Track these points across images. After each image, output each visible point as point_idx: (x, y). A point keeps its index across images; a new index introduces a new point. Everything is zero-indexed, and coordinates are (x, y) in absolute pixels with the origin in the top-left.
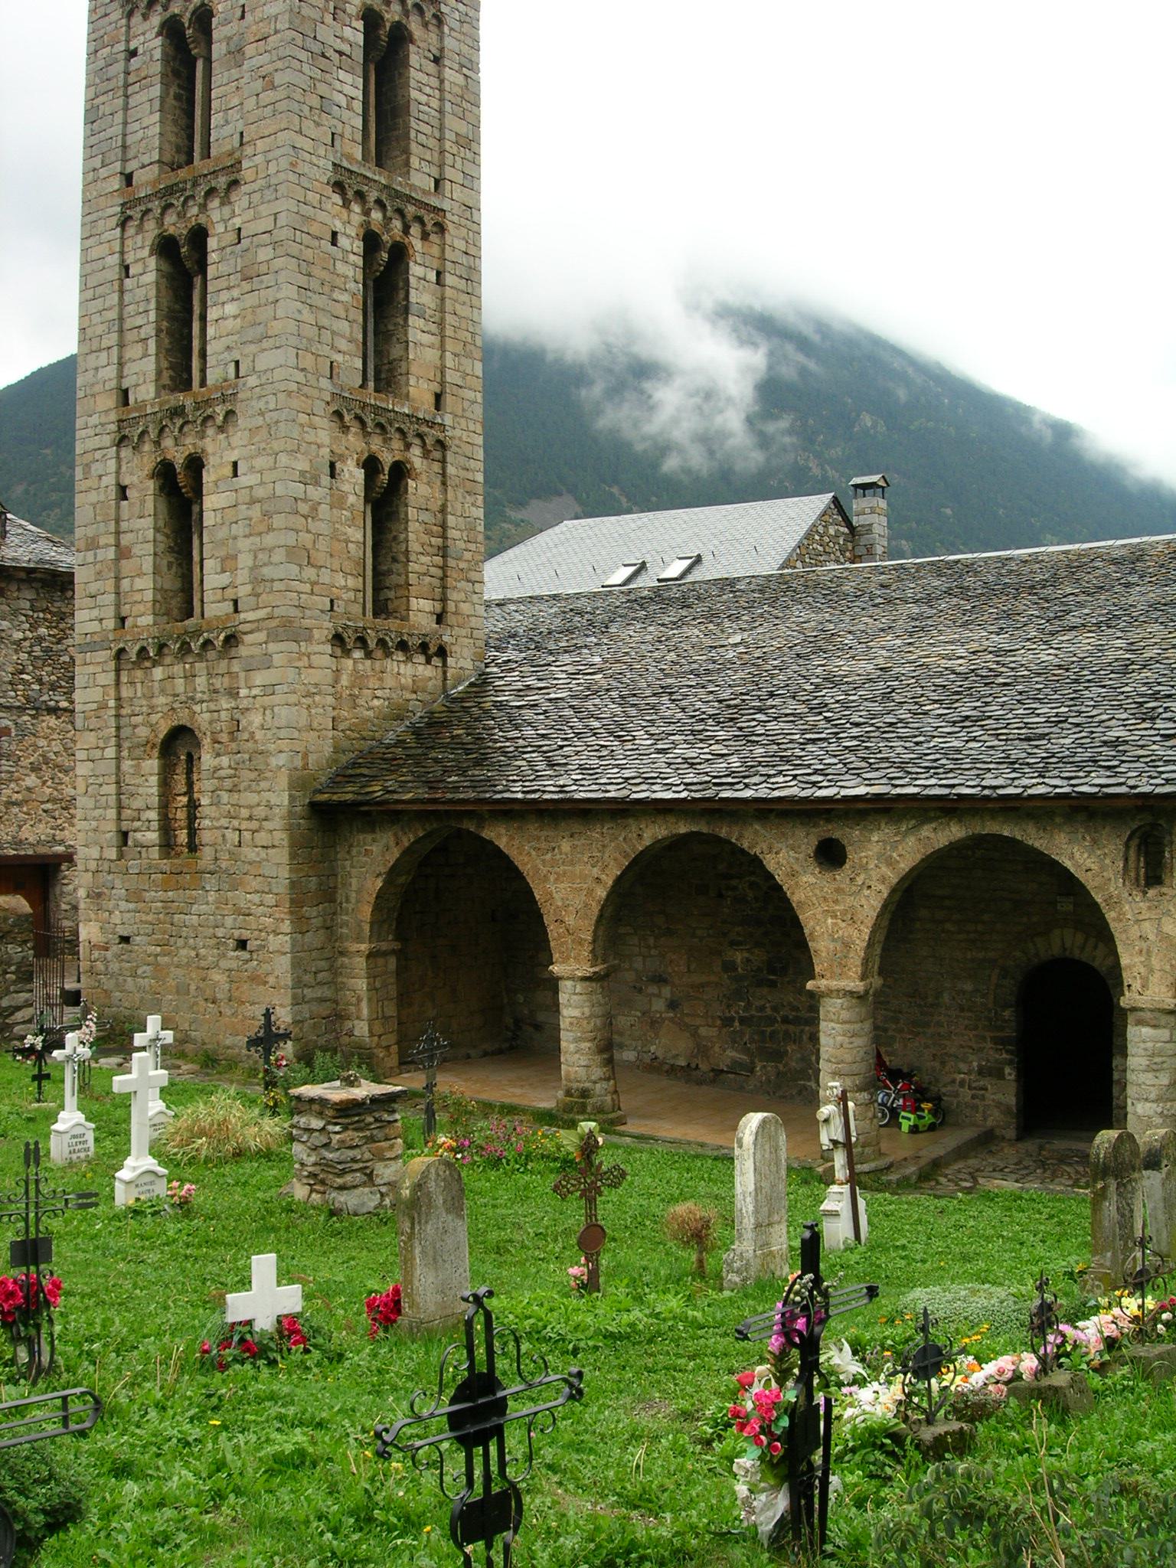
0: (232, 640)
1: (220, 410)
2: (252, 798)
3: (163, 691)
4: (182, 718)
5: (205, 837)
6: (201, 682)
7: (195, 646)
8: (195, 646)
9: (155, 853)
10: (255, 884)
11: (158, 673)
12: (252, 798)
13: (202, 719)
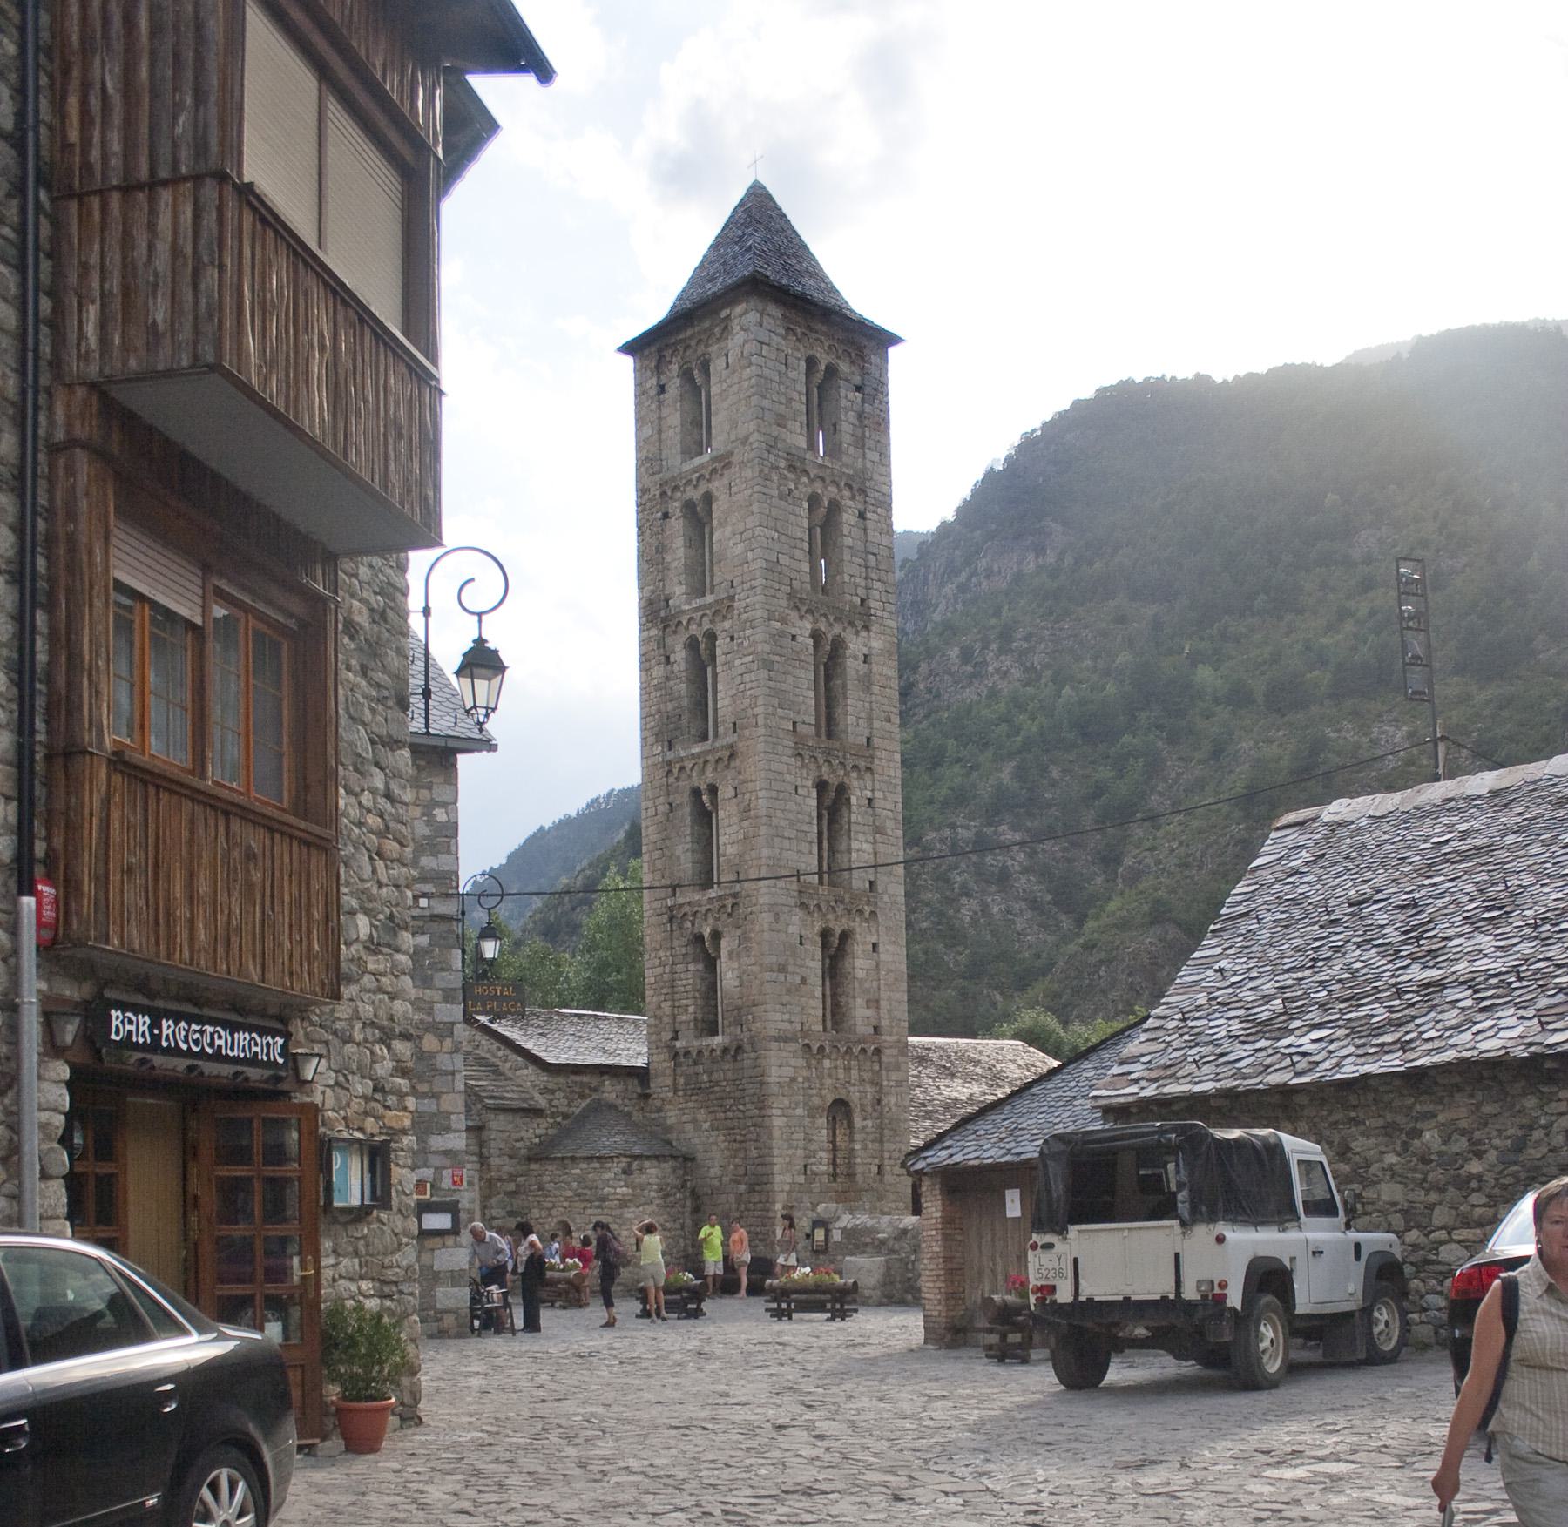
0: (878, 1051)
1: (867, 910)
2: (892, 1147)
3: (830, 1076)
4: (842, 1095)
5: (859, 1169)
6: (854, 1072)
7: (856, 1050)
8: (856, 1050)
9: (825, 1179)
10: (892, 1197)
11: (827, 1063)
12: (892, 1147)
13: (854, 1097)
